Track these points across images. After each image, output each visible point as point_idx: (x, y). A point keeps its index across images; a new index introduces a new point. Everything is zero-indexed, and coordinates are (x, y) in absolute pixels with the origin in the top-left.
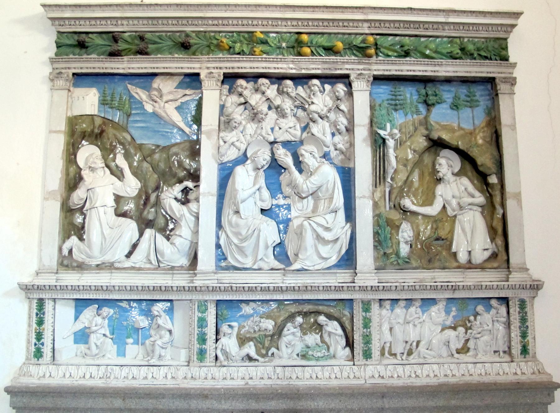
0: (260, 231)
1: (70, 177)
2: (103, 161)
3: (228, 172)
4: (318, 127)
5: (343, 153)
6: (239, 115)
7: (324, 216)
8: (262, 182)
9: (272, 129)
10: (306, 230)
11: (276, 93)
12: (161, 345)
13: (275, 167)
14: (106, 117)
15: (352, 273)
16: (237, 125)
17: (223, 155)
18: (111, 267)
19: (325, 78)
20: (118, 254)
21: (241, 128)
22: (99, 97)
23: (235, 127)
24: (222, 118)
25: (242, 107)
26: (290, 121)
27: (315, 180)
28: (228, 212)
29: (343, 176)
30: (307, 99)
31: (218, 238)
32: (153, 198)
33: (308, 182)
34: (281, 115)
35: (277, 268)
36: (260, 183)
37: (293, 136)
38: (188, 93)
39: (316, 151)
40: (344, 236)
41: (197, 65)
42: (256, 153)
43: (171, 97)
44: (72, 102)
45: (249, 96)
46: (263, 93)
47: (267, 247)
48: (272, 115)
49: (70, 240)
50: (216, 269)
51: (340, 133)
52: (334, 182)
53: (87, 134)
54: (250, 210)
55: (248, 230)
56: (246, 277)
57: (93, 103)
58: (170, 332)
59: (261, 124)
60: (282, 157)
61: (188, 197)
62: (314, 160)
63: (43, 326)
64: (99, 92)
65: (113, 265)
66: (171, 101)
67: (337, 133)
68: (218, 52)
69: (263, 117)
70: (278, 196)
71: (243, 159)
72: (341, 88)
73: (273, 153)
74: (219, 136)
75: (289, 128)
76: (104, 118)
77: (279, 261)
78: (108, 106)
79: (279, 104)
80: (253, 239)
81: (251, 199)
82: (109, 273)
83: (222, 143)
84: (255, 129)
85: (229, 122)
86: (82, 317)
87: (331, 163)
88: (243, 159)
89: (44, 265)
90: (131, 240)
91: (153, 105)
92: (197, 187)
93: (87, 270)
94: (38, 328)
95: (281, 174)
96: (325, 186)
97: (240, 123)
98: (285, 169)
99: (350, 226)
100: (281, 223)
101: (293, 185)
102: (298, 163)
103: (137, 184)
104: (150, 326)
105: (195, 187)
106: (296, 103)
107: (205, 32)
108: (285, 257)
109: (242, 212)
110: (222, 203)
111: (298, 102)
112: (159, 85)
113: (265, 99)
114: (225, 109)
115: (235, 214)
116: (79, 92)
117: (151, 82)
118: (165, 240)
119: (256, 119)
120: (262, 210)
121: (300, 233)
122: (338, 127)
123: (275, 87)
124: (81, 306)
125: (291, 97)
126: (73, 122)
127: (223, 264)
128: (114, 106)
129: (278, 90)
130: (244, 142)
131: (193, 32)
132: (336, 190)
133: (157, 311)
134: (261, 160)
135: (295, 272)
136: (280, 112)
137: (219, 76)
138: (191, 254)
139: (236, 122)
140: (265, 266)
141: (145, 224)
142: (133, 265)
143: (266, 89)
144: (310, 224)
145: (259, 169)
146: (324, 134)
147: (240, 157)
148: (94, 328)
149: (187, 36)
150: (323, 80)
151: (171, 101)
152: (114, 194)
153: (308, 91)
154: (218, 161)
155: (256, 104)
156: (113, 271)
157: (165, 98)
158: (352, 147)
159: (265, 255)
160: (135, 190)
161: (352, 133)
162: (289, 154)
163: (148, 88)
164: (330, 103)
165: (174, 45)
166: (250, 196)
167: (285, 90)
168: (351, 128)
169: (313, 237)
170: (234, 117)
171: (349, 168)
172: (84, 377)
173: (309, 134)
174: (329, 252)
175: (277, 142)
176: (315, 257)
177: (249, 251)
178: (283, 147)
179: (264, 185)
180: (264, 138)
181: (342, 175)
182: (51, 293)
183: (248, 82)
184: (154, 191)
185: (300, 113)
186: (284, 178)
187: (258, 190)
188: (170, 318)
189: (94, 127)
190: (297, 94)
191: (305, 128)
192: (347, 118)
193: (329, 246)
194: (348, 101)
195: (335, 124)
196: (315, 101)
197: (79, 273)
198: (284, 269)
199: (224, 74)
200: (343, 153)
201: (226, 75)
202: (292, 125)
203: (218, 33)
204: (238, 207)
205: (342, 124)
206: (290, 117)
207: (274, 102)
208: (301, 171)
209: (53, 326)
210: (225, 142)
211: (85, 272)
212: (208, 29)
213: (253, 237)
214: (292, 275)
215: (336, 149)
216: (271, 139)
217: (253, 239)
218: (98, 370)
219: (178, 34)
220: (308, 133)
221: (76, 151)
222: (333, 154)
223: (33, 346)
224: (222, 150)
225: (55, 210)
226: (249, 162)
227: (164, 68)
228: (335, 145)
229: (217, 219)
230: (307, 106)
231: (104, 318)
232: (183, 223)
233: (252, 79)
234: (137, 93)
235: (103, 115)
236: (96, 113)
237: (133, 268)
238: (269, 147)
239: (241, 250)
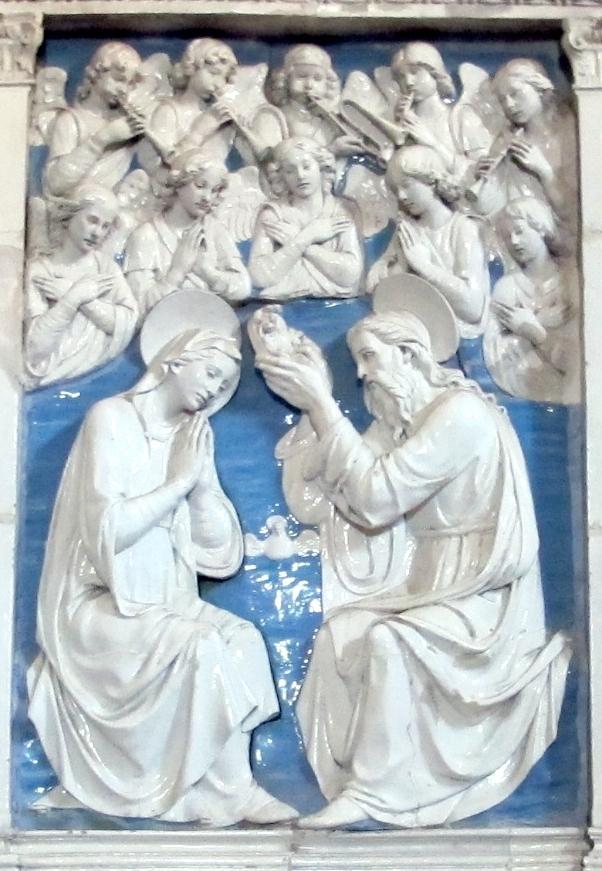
0: (194, 666)
3: (64, 423)
4: (432, 239)
5: (535, 346)
6: (107, 189)
7: (456, 605)
8: (203, 464)
9: (245, 248)
10: (383, 664)
11: (262, 99)
13: (258, 404)
15: (571, 838)
16: (99, 231)
17: (45, 356)
19: (459, 39)
21: (117, 244)
23: (93, 241)
24: (39, 204)
25: (122, 157)
26: (319, 216)
27: (421, 458)
28: (62, 586)
29: (537, 442)
30: (390, 125)
31: (22, 694)
33: (390, 464)
34: (279, 188)
35: (264, 818)
36: (196, 467)
37: (328, 276)
39: (424, 336)
40: (538, 688)
42: (178, 345)
45: (148, 111)
46: (209, 100)
47: (223, 733)
48: (245, 189)
50: (14, 823)
51: (523, 266)
52: (501, 465)
54: (153, 579)
55: (146, 663)
56: (139, 854)
59: (198, 227)
60: (285, 361)
62: (418, 375)
67: (510, 265)
69: (209, 196)
70: (270, 521)
71: (126, 369)
72: (527, 78)
73: (247, 348)
74: (24, 276)
75: (316, 243)
77: (272, 789)
79: (273, 144)
80: (166, 702)
81: (158, 535)
83: (37, 305)
84: (172, 246)
85: (66, 219)
87: (486, 389)
88: (126, 369)
95: (280, 431)
96: (461, 483)
97: (114, 224)
98: (297, 411)
99: (566, 644)
100: (281, 634)
101: (330, 477)
102: (353, 390)
106: (343, 142)
108: (295, 775)
109: (119, 587)
110: (40, 553)
111: (352, 137)
113: (214, 123)
114: (51, 165)
115: (91, 597)
119: (178, 208)
120: (206, 584)
121: (359, 677)
122: (516, 239)
123: (258, 73)
125: (323, 116)
127: (44, 803)
129: (269, 85)
130: (130, 301)
132: (508, 499)
134: (200, 374)
135: (339, 834)
136: (279, 178)
137: (27, 28)
139: (95, 220)
140: (217, 812)
143: (220, 81)
144: (400, 639)
145: (190, 412)
146: (457, 269)
147: (110, 361)
150: (453, 46)
153: (393, 91)
154: (24, 378)
155: (179, 145)
158: (574, 325)
159: (214, 766)
161: (573, 262)
162: (314, 350)
164: (482, 140)
166: (155, 524)
167: (298, 85)
168: (571, 243)
169: (413, 692)
170: (90, 197)
171: (563, 410)
173: (398, 269)
174: (478, 755)
175: (262, 302)
176: (423, 776)
177: (149, 750)
178: (291, 322)
179: (210, 477)
180: (211, 285)
181: (530, 436)
183: (144, 54)
185: (360, 180)
186: (293, 450)
187: (187, 496)
190: (348, 103)
191: (381, 244)
192: (551, 203)
193: (480, 728)
194: (555, 131)
195: (501, 228)
196: (420, 130)
198: (294, 825)
199: (48, 20)
200: (535, 346)
201: (55, 27)
202: (324, 229)
204: (104, 570)
205: (533, 226)
206: (317, 198)
207: (251, 135)
208: (362, 421)
210: (51, 302)
213: (167, 692)
214: (324, 849)
215: (507, 332)
216: (242, 288)
217: (166, 702)
220: (391, 264)
222: (497, 349)
224: (39, 335)
226: (148, 381)
228: (502, 314)
229: (16, 618)
230: (387, 154)
233: (160, 42)
238: (231, 320)
239: (115, 744)
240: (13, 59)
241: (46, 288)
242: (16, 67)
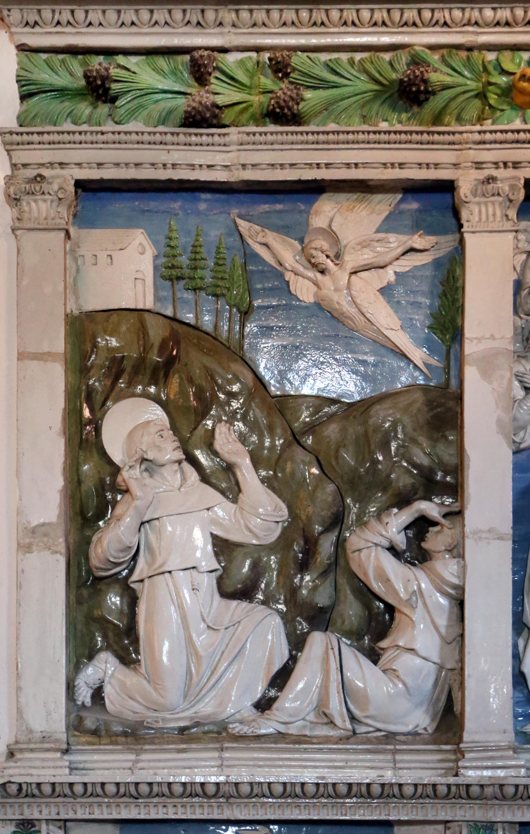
1: (84, 488)
2: (177, 444)
14: (179, 316)
18: (219, 733)
20: (235, 697)
22: (156, 258)
32: (326, 546)
38: (417, 246)
41: (446, 156)
43: (366, 257)
44: (78, 271)
49: (95, 662)
53: (128, 365)
57: (139, 276)
61: (423, 545)
64: (155, 243)
65: (226, 729)
66: (367, 268)
68: (509, 112)
76: (174, 319)
78: (182, 283)
82: (216, 749)
89: (31, 731)
90: (270, 662)
91: (316, 284)
92: (456, 515)
93: (153, 743)
103: (276, 508)
105: (445, 516)
107: (469, 49)
112: (331, 221)
116: (95, 240)
117: (308, 213)
118: (366, 663)
126: (83, 328)
128: (199, 283)
131: (433, 48)
137: (513, 187)
138: (438, 699)
141: (307, 618)
142: (282, 729)
149: (416, 61)
151: (367, 268)
152: (212, 534)
156: (226, 745)
157: (351, 260)
160: (273, 525)
163: (298, 232)
165: (377, 94)
182: (57, 805)
184: (327, 530)
189: (146, 348)
197: (130, 751)
203: (507, 54)
211: (147, 747)
212: (483, 39)
219: (387, 56)
221: (99, 415)
225: (51, 572)
227: (348, 165)
232: (418, 615)
234: (266, 245)
235: (169, 312)
236: (149, 304)
237: (280, 737)
240: (502, 212)
241: (525, 380)
242: (505, 218)
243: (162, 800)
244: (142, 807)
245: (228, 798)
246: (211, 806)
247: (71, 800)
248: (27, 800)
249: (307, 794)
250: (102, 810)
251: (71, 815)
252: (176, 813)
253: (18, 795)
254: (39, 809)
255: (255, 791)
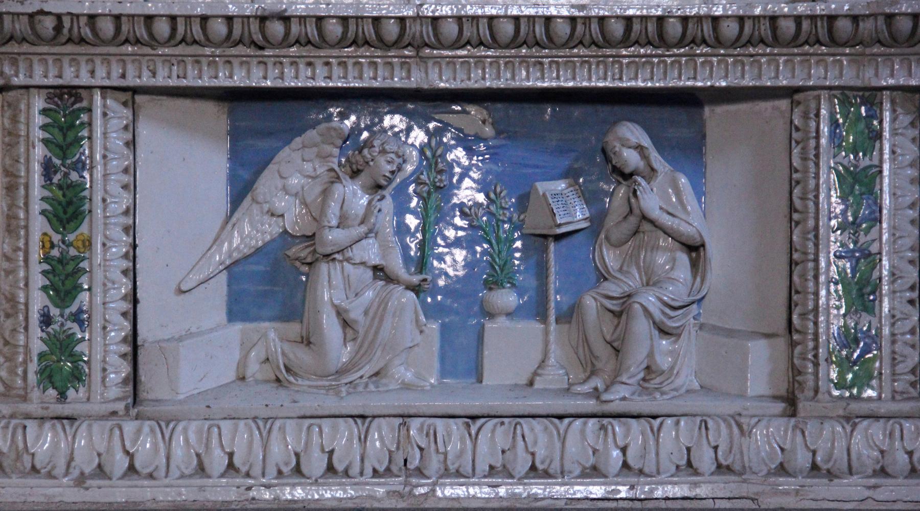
12: (657, 315)
58: (694, 249)
63: (84, 229)
86: (267, 183)
94: (56, 238)
104: (597, 221)
124: (269, 134)
133: (640, 148)
148: (334, 237)
172: (298, 470)
188: (694, 188)
209: (131, 230)
218: (363, 440)
223: (36, 332)
231: (377, 187)
243: (304, 51)
244: (270, 66)
245: (418, 48)
246: (390, 63)
247: (148, 50)
248: (69, 48)
249: (555, 39)
250: (200, 71)
251: (146, 80)
252: (329, 78)
253: (55, 38)
254: (90, 67)
255: (467, 34)
